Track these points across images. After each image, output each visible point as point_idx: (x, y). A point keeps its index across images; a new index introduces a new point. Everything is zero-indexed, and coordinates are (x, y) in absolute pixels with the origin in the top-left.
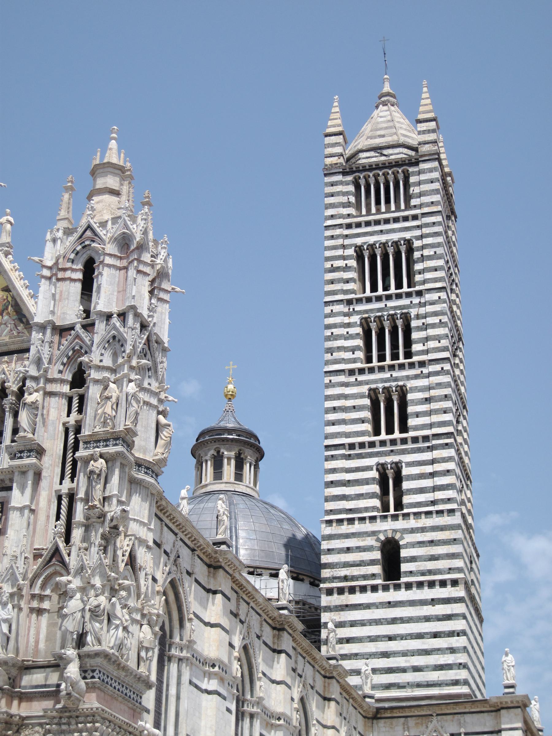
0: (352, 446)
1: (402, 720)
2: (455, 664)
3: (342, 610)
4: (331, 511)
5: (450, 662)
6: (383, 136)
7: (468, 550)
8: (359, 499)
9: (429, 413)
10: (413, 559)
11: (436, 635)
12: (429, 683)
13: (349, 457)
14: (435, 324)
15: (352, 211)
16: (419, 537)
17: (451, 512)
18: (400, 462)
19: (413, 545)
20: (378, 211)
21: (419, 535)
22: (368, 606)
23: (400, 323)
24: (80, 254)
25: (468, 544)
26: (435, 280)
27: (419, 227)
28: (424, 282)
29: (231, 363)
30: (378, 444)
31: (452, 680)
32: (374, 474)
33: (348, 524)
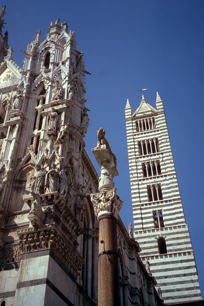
0: (143, 205)
2: (195, 287)
4: (137, 228)
5: (193, 286)
6: (144, 110)
8: (147, 224)
11: (184, 275)
12: (185, 296)
14: (169, 163)
16: (173, 236)
18: (161, 210)
19: (170, 239)
21: (172, 236)
23: (156, 164)
24: (43, 52)
26: (168, 149)
27: (159, 134)
31: (195, 294)
32: (151, 215)
33: (144, 233)
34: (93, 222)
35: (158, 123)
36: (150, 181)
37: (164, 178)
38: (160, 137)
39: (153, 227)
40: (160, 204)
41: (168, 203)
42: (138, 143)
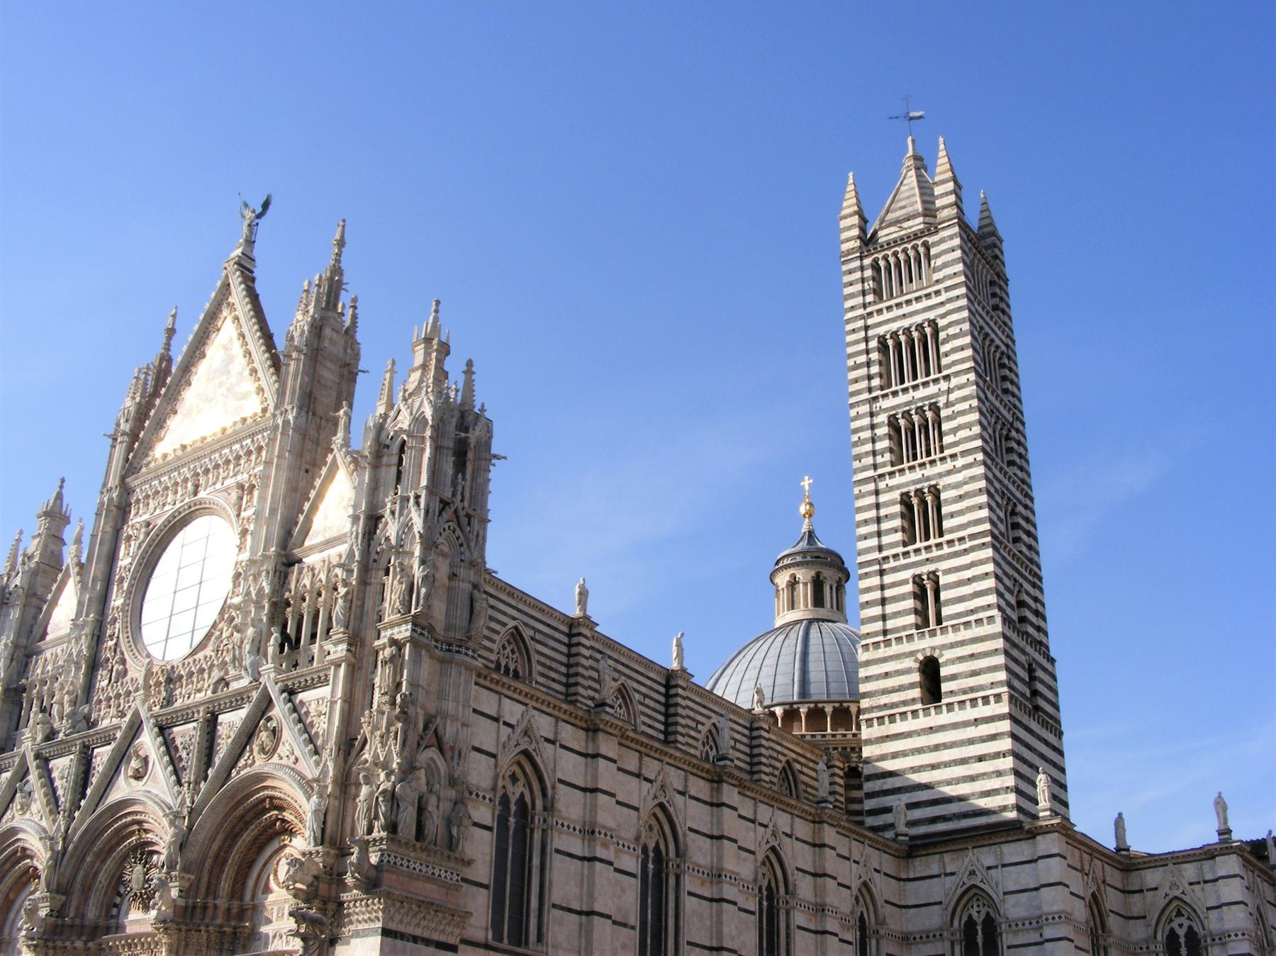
0: (886, 559)
1: (938, 856)
3: (884, 742)
6: (904, 207)
7: (1022, 658)
10: (953, 677)
11: (981, 759)
17: (991, 619)
18: (937, 570)
20: (902, 294)
22: (908, 735)
25: (1023, 652)
26: (963, 361)
27: (942, 304)
28: (954, 363)
29: (806, 478)
30: (912, 554)
32: (909, 588)
33: (885, 646)
34: (544, 795)
35: (939, 262)
36: (909, 479)
37: (949, 465)
38: (943, 316)
39: (911, 625)
40: (935, 553)
41: (958, 547)
42: (879, 342)
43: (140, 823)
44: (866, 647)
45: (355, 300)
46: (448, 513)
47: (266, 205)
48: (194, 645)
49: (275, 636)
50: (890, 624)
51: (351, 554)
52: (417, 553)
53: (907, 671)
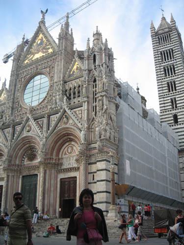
0: (164, 95)
9: (180, 86)
10: (180, 118)
13: (164, 98)
15: (158, 44)
19: (180, 115)
23: (172, 67)
32: (170, 101)
35: (172, 37)
37: (177, 77)
43: (29, 141)
44: (161, 112)
45: (72, 29)
46: (108, 69)
47: (47, 11)
48: (40, 102)
49: (65, 98)
50: (166, 108)
51: (85, 78)
52: (104, 76)
53: (171, 117)
